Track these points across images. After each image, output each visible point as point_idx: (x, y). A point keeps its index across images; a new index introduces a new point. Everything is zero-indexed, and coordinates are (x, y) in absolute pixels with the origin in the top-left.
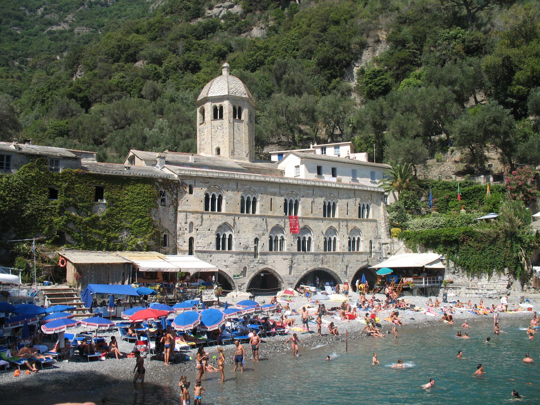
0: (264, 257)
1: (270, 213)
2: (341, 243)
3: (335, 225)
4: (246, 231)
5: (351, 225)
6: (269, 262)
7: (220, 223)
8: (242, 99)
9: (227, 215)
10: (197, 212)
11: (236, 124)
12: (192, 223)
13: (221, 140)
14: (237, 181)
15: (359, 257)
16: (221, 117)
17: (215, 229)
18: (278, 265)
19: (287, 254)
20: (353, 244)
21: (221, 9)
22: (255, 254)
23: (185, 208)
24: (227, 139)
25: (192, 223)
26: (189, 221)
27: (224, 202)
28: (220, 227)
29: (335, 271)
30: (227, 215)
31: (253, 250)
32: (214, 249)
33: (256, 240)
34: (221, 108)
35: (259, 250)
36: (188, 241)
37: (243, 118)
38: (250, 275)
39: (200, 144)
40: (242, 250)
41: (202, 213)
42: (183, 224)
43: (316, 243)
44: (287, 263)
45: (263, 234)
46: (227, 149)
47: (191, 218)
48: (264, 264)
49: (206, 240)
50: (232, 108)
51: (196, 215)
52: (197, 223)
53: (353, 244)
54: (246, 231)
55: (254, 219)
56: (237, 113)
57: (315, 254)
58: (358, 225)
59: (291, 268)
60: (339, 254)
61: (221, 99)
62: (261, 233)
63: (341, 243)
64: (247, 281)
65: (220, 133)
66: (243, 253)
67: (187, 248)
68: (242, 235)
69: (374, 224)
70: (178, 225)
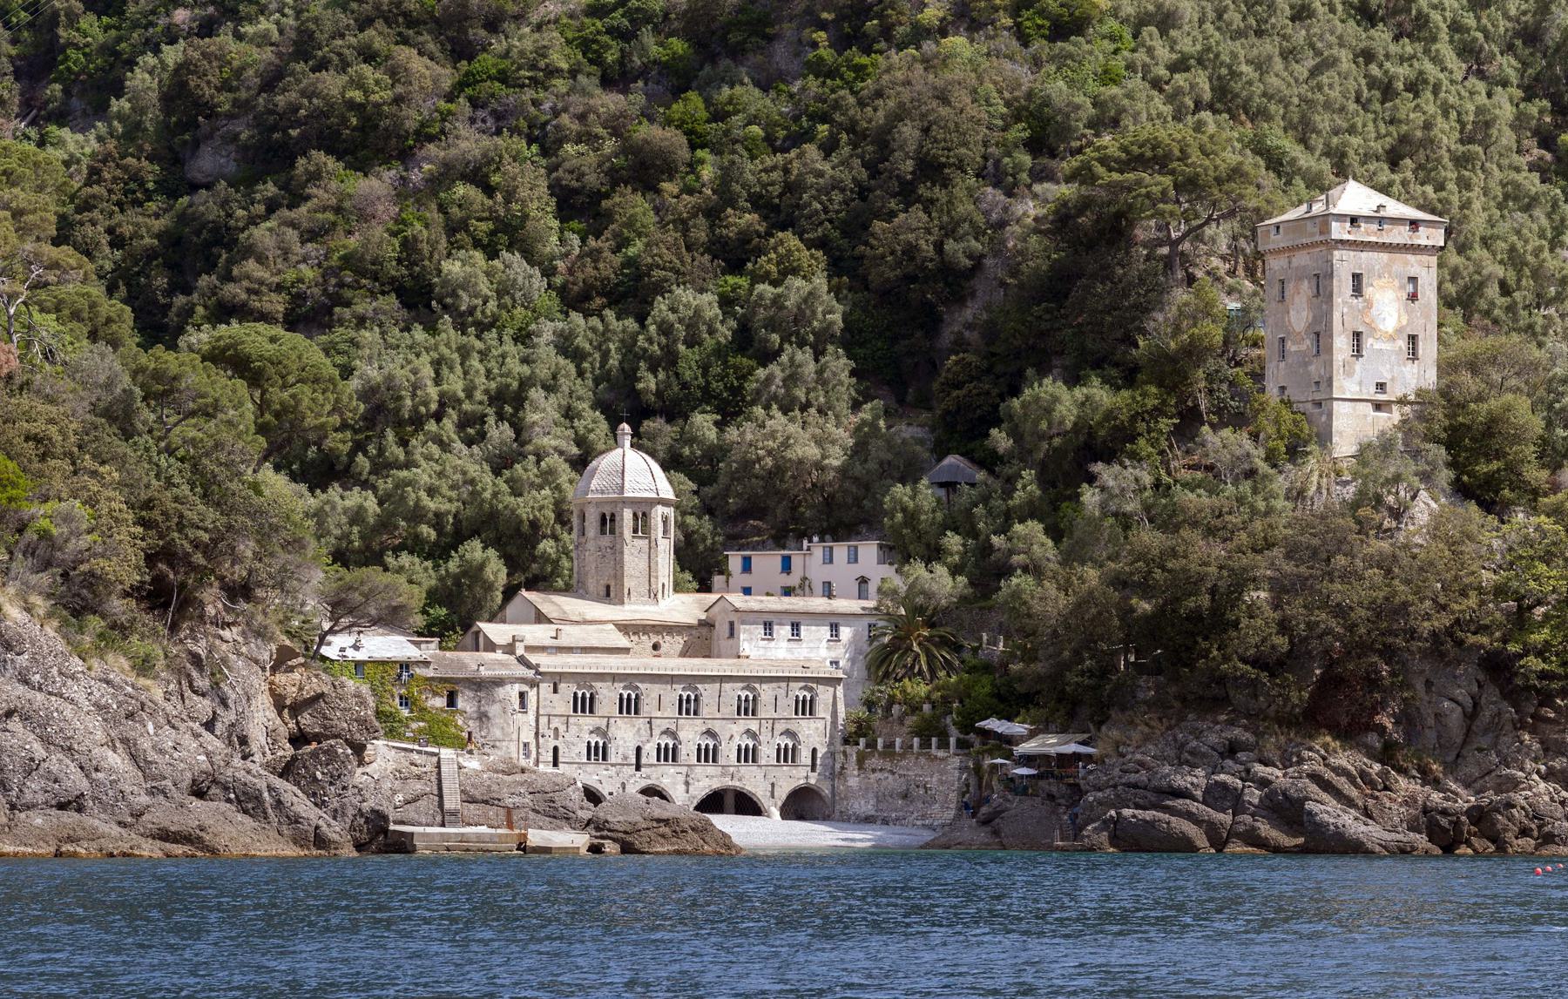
1: (659, 714)
4: (626, 735)
22: (638, 768)
23: (549, 711)
31: (634, 761)
33: (639, 750)
35: (644, 760)
43: (728, 753)
44: (681, 778)
47: (556, 723)
48: (648, 777)
49: (574, 749)
52: (562, 729)
54: (626, 735)
58: (793, 726)
59: (687, 784)
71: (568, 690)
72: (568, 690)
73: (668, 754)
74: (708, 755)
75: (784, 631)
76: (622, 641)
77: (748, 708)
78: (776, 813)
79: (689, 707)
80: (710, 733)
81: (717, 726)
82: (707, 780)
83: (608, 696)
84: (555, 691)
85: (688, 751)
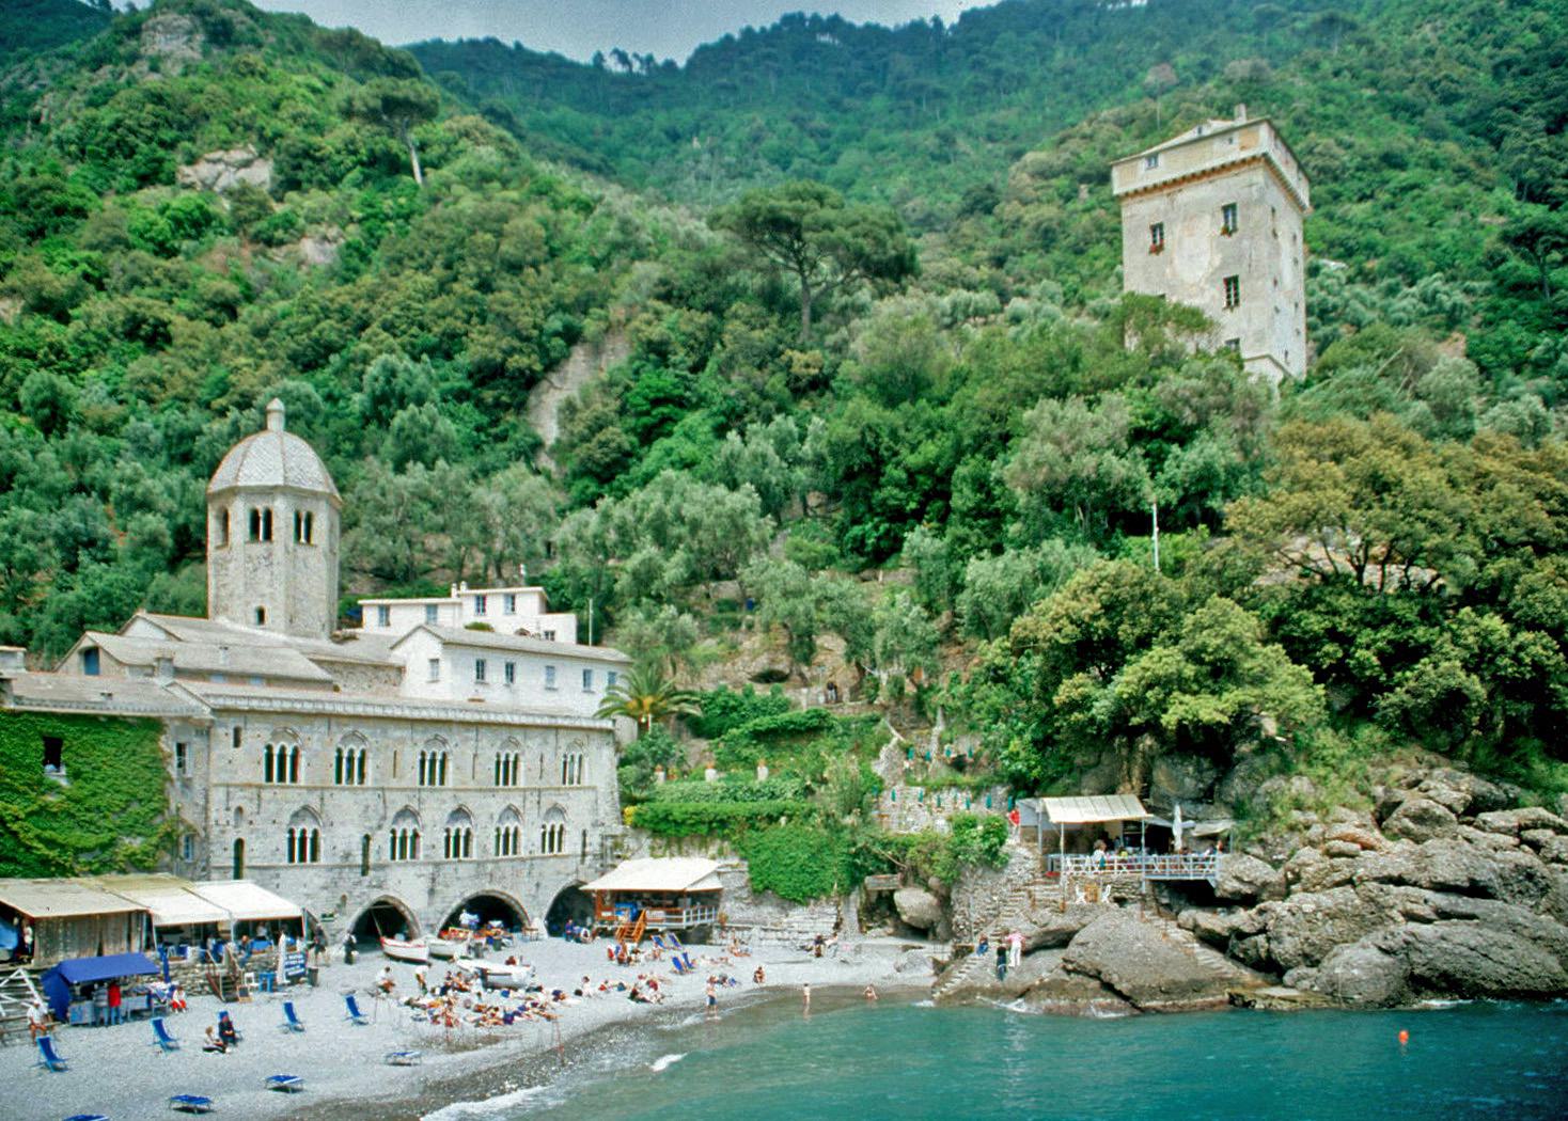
0: (381, 874)
1: (394, 783)
2: (530, 839)
3: (517, 802)
5: (548, 801)
6: (390, 883)
7: (296, 807)
8: (315, 495)
9: (310, 789)
10: (250, 786)
11: (302, 552)
12: (240, 810)
13: (267, 591)
14: (329, 717)
15: (560, 865)
16: (268, 536)
17: (286, 818)
18: (407, 888)
19: (426, 864)
20: (553, 839)
21: (221, 167)
22: (365, 869)
23: (225, 777)
24: (280, 588)
25: (240, 810)
26: (234, 805)
27: (302, 762)
28: (296, 815)
29: (516, 896)
30: (310, 789)
31: (359, 860)
32: (285, 862)
34: (268, 515)
35: (372, 860)
36: (231, 847)
37: (313, 541)
38: (355, 912)
39: (217, 596)
40: (338, 861)
41: (260, 787)
42: (223, 813)
44: (423, 884)
45: (380, 827)
46: (280, 612)
48: (380, 887)
49: (267, 845)
50: (292, 516)
51: (248, 793)
52: (249, 808)
53: (553, 839)
55: (361, 796)
56: (303, 525)
57: (479, 863)
58: (562, 802)
59: (432, 892)
60: (523, 860)
61: (269, 491)
62: (374, 823)
63: (530, 839)
64: (346, 922)
65: (264, 575)
66: (341, 867)
67: (231, 863)
68: (339, 830)
69: (591, 795)
70: (213, 815)
71: (257, 738)
72: (257, 738)
73: (405, 846)
74: (458, 845)
75: (495, 674)
76: (319, 673)
77: (506, 771)
78: (538, 923)
79: (433, 769)
80: (460, 813)
81: (472, 802)
82: (462, 885)
83: (317, 752)
84: (237, 743)
85: (432, 839)
